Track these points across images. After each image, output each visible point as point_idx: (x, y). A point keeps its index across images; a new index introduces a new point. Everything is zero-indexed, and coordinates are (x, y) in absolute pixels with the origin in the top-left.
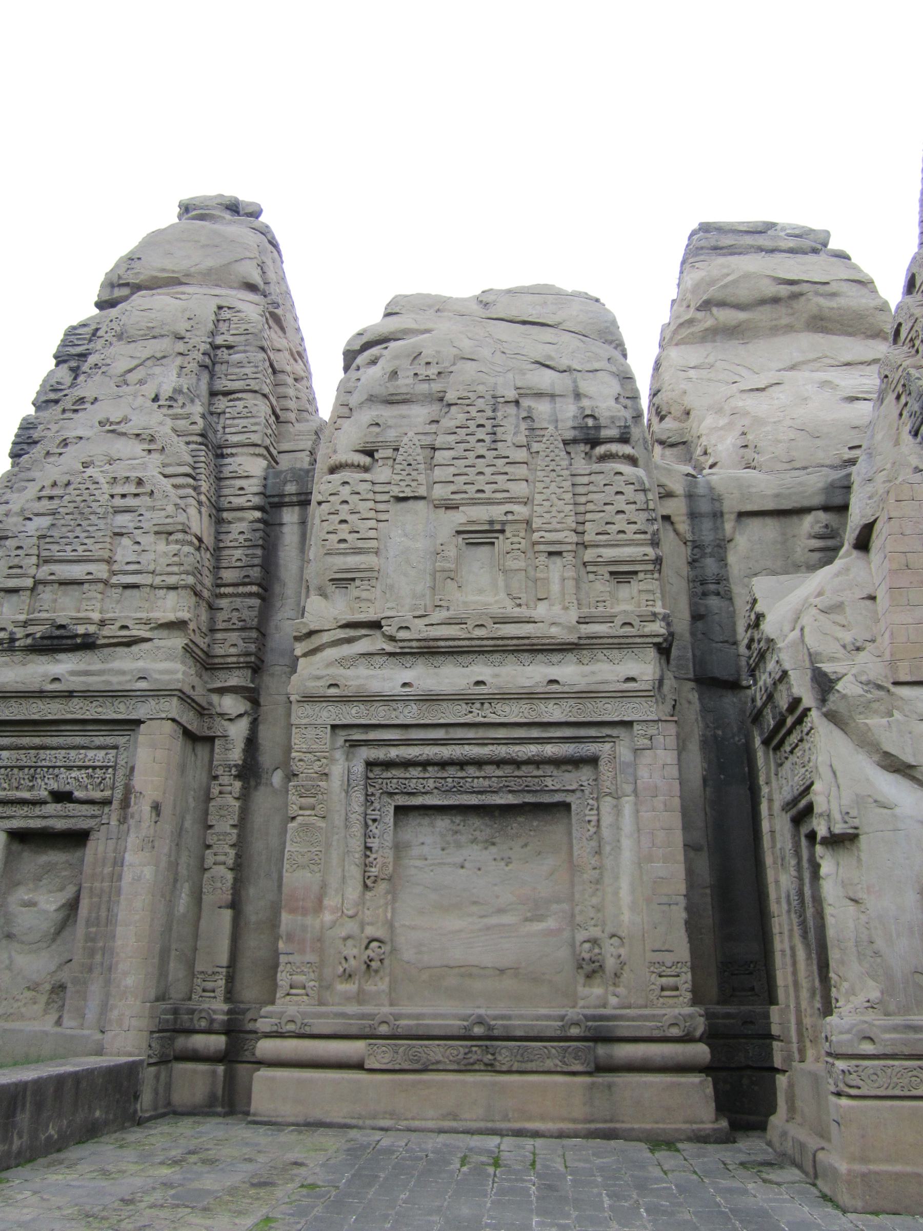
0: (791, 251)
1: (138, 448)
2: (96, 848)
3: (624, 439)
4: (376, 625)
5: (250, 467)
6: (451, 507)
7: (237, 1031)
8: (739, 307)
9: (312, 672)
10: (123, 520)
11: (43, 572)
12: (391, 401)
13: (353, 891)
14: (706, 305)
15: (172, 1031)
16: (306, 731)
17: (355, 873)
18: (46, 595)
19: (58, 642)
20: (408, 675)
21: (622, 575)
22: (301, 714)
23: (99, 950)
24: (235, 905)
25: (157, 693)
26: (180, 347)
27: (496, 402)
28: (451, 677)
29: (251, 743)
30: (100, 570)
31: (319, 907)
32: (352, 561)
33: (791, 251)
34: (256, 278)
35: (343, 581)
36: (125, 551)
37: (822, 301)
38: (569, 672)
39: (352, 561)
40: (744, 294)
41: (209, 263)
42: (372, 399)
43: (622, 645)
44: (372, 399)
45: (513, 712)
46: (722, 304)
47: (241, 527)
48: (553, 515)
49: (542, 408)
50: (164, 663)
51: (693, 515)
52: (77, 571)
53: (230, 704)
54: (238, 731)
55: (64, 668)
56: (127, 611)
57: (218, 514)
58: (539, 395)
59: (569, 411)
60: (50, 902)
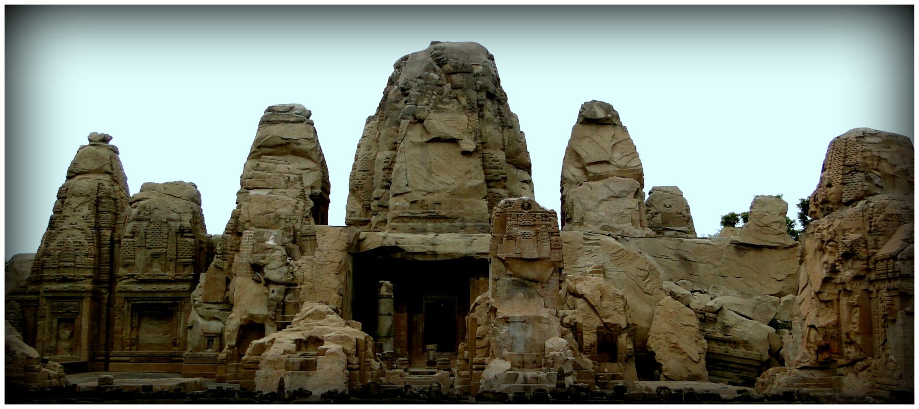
0: (294, 122)
2: (77, 322)
3: (190, 232)
4: (133, 276)
5: (107, 233)
6: (150, 248)
7: (107, 356)
8: (270, 147)
9: (120, 285)
10: (77, 252)
11: (61, 264)
12: (138, 220)
13: (129, 330)
14: (259, 147)
15: (93, 358)
16: (119, 301)
17: (129, 326)
18: (61, 269)
19: (65, 280)
20: (140, 287)
21: (185, 265)
22: (117, 295)
23: (78, 341)
24: (107, 332)
25: (87, 291)
26: (89, 199)
27: (162, 222)
28: (149, 287)
29: (109, 298)
30: (73, 264)
31: (122, 333)
32: (129, 261)
33: (294, 122)
34: (110, 170)
35: (126, 266)
36: (78, 260)
37: (295, 146)
38: (173, 287)
39: (129, 261)
40: (271, 143)
41: (96, 167)
42: (134, 219)
44: (134, 219)
45: (161, 295)
46: (264, 147)
47: (106, 249)
48: (171, 253)
49: (173, 224)
50: (88, 285)
51: (208, 247)
52: (68, 264)
53: (104, 291)
54: (106, 296)
55: (66, 285)
56: (80, 273)
57: (100, 245)
58: (172, 220)
59: (178, 224)
60: (68, 332)
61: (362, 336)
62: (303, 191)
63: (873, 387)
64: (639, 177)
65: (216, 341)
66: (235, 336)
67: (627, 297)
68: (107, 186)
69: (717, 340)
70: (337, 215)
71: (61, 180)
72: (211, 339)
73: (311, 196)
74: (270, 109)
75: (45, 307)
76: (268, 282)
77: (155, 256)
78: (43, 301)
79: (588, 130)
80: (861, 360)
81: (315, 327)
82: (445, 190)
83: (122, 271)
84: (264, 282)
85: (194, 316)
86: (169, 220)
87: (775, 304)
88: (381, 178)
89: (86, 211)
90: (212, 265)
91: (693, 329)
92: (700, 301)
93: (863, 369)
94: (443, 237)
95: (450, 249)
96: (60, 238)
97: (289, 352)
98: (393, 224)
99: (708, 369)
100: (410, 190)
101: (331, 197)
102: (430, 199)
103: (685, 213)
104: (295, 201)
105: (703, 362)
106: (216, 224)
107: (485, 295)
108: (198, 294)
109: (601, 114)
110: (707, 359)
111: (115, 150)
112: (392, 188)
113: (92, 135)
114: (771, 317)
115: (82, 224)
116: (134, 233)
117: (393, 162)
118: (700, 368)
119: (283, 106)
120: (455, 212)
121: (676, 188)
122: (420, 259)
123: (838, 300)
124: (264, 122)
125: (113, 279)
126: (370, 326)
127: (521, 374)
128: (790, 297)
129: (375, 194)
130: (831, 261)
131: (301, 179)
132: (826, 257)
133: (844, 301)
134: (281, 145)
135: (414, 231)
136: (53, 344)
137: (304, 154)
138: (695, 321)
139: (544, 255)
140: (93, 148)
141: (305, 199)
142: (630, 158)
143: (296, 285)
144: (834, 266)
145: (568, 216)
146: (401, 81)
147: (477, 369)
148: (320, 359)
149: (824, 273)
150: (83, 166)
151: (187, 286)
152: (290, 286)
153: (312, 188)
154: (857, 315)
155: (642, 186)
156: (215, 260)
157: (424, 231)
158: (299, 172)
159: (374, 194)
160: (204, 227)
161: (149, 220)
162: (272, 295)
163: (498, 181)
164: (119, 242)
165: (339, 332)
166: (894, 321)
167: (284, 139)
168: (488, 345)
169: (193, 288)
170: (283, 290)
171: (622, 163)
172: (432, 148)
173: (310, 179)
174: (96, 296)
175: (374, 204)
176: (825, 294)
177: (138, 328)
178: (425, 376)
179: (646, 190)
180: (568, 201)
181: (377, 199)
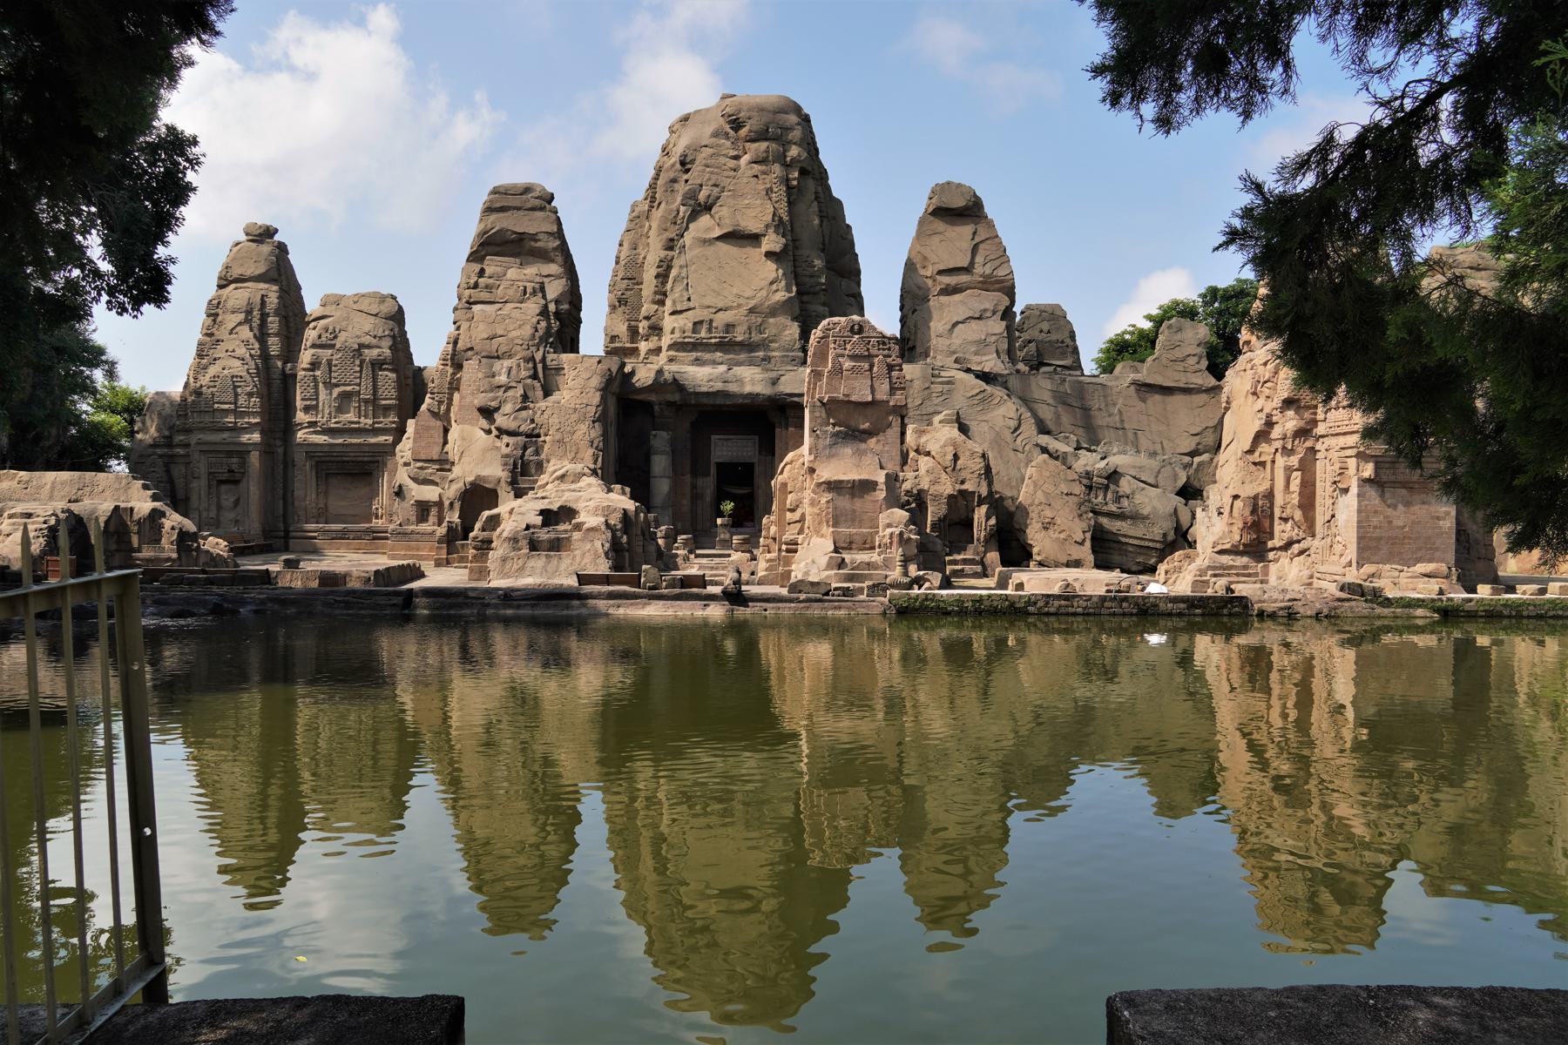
1: (238, 363)
6: (337, 385)
7: (287, 532)
9: (301, 435)
15: (267, 532)
16: (299, 457)
24: (285, 499)
29: (285, 453)
42: (314, 346)
43: (384, 431)
44: (314, 346)
48: (366, 394)
54: (280, 451)
55: (226, 435)
61: (631, 505)
62: (546, 306)
63: (1311, 577)
64: (1010, 292)
65: (434, 511)
66: (457, 505)
67: (990, 455)
68: (273, 299)
69: (1110, 515)
70: (592, 340)
71: (211, 290)
72: (423, 509)
73: (557, 314)
74: (495, 191)
75: (201, 466)
76: (502, 432)
77: (346, 396)
78: (196, 456)
79: (939, 225)
80: (1299, 542)
81: (567, 494)
82: (739, 306)
83: (301, 417)
84: (495, 432)
85: (403, 477)
86: (361, 346)
87: (1187, 466)
88: (653, 289)
89: (246, 333)
90: (424, 407)
91: (1076, 499)
92: (1088, 461)
93: (1301, 553)
94: (738, 370)
95: (748, 389)
96: (212, 371)
97: (535, 526)
98: (671, 353)
99: (1094, 552)
100: (691, 304)
101: (582, 315)
102: (721, 319)
103: (1068, 341)
104: (535, 320)
105: (1088, 544)
106: (427, 352)
107: (797, 452)
108: (405, 449)
109: (959, 202)
110: (1093, 539)
111: (282, 249)
112: (668, 302)
113: (248, 226)
114: (1180, 483)
115: (241, 351)
116: (314, 365)
117: (669, 268)
118: (1086, 553)
119: (515, 186)
120: (756, 337)
121: (1058, 306)
122: (705, 401)
123: (1273, 462)
124: (489, 210)
125: (289, 427)
126: (641, 493)
127: (847, 557)
128: (1206, 457)
129: (643, 312)
130: (1267, 410)
131: (542, 289)
132: (1260, 403)
133: (1281, 461)
134: (513, 241)
135: (698, 362)
136: (213, 514)
137: (543, 256)
138: (1078, 489)
139: (879, 397)
140: (254, 245)
141: (548, 319)
142: (997, 263)
143: (538, 436)
144: (1269, 416)
145: (911, 344)
146: (678, 151)
147: (788, 551)
148: (576, 535)
149: (1257, 425)
150: (236, 272)
151: (390, 439)
152: (532, 435)
153: (557, 302)
154: (1298, 481)
155: (1013, 303)
156: (427, 400)
157: (715, 363)
158: (538, 279)
159: (643, 312)
160: (409, 356)
161: (333, 346)
162: (506, 451)
163: (815, 293)
164: (295, 376)
165: (599, 503)
166: (1346, 491)
167: (518, 233)
168: (802, 520)
169: (398, 440)
170: (521, 444)
171: (988, 271)
172: (723, 247)
173: (555, 289)
174: (267, 449)
175: (643, 326)
176: (1257, 454)
177: (326, 494)
178: (717, 560)
179: (1017, 309)
180: (911, 323)
181: (648, 318)
